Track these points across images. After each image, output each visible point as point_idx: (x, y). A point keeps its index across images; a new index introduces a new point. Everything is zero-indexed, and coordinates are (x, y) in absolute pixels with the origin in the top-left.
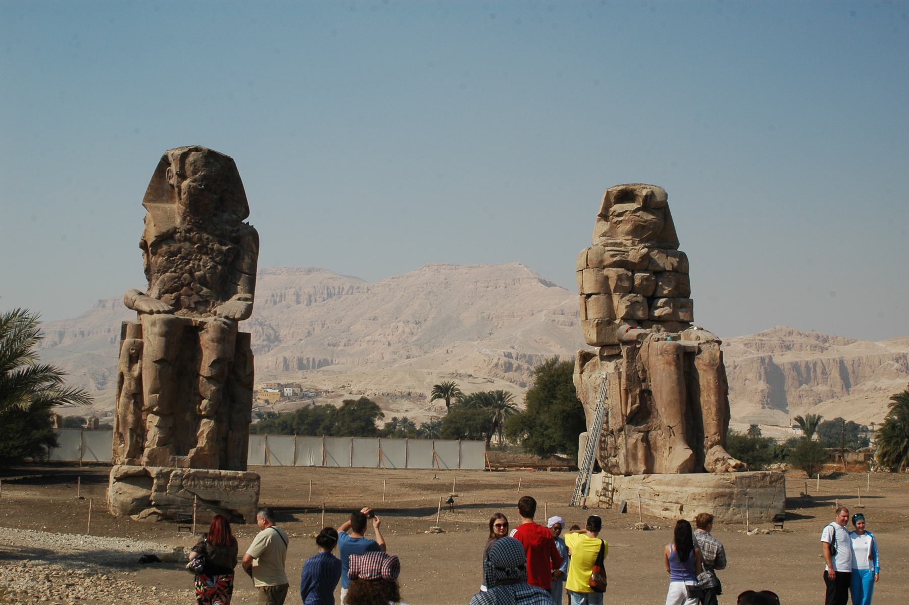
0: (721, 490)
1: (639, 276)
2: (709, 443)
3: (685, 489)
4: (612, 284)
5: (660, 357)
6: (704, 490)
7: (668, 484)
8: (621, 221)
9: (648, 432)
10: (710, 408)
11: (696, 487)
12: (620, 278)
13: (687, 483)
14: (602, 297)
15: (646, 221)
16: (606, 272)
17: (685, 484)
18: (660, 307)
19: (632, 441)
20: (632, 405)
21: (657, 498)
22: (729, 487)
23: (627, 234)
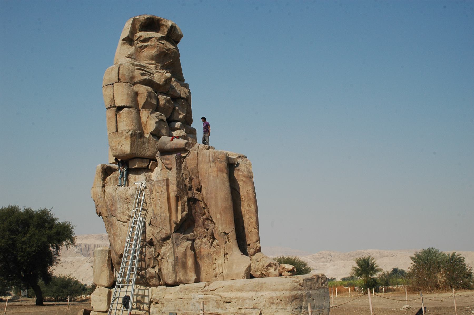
0: (295, 293)
1: (162, 98)
2: (253, 250)
3: (260, 293)
4: (141, 101)
5: (212, 164)
6: (282, 293)
7: (241, 290)
8: (146, 47)
9: (193, 241)
10: (250, 217)
11: (273, 290)
12: (149, 94)
13: (262, 287)
14: (133, 111)
15: (169, 50)
16: (136, 88)
17: (260, 288)
18: (177, 129)
19: (181, 249)
20: (182, 212)
21: (228, 305)
22: (300, 289)
23: (152, 59)
